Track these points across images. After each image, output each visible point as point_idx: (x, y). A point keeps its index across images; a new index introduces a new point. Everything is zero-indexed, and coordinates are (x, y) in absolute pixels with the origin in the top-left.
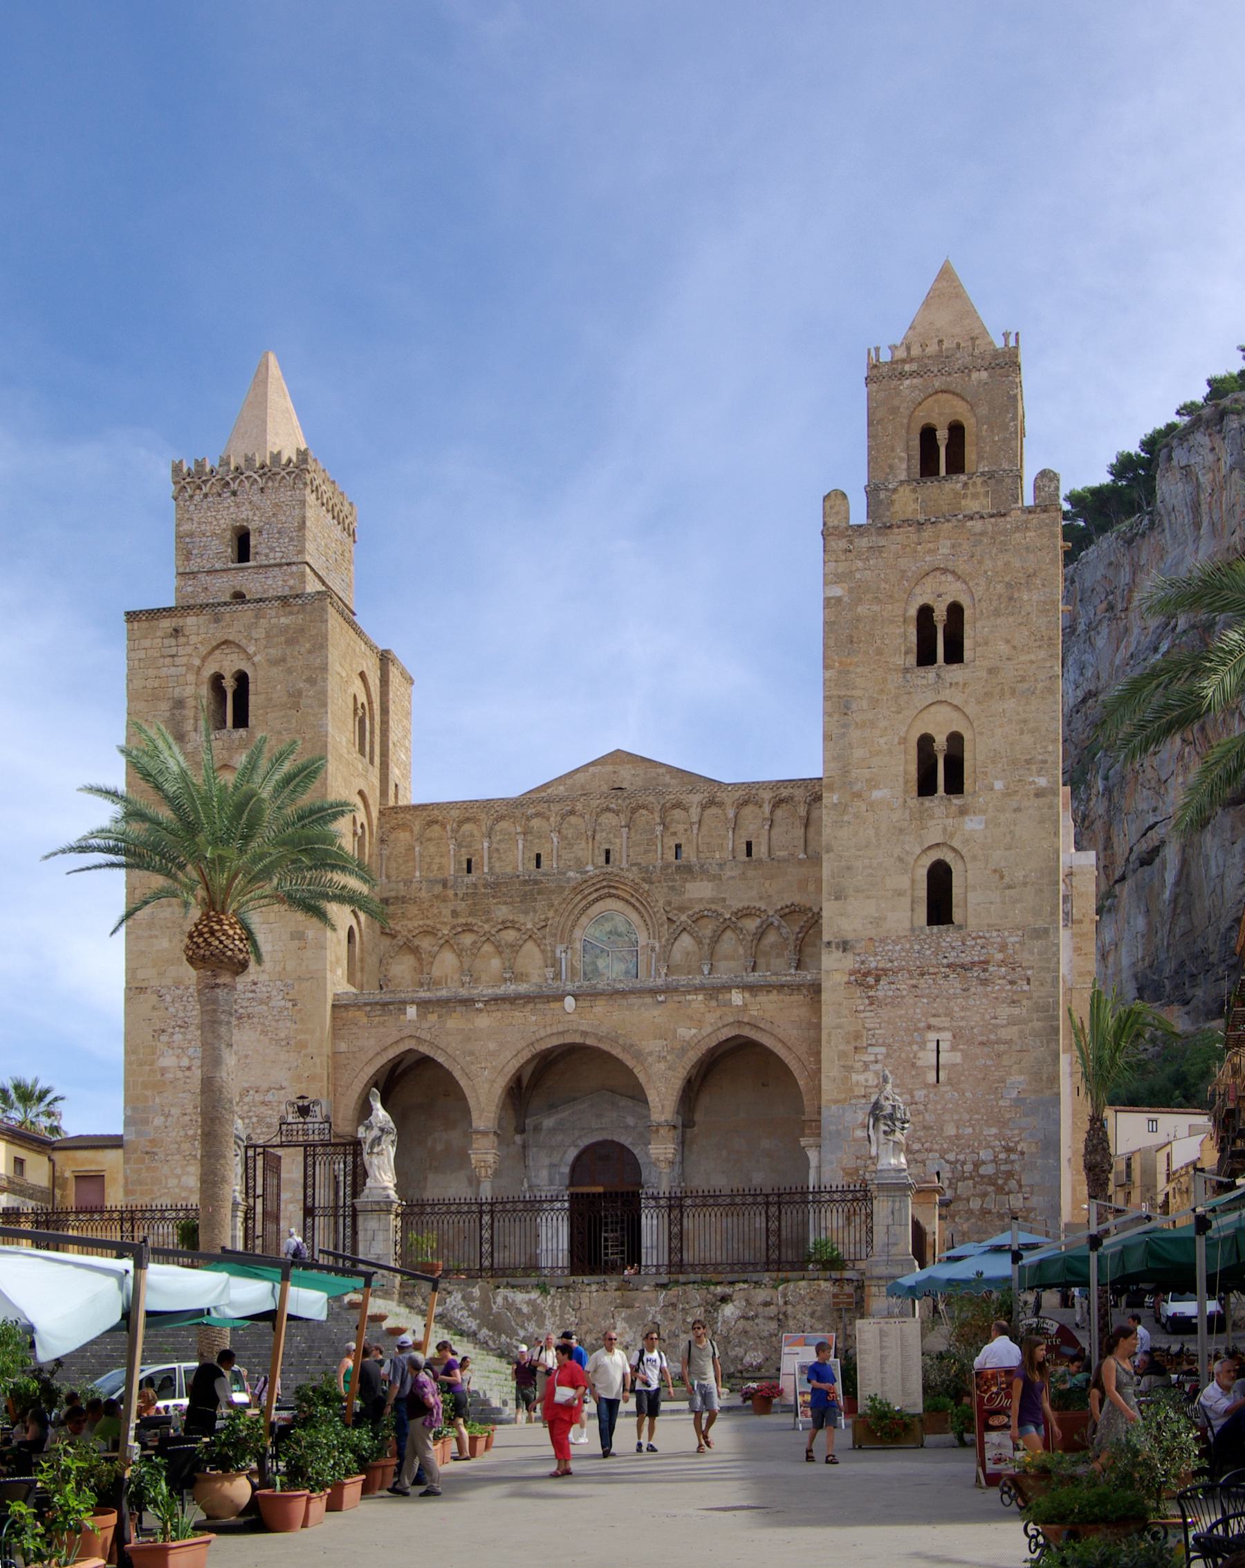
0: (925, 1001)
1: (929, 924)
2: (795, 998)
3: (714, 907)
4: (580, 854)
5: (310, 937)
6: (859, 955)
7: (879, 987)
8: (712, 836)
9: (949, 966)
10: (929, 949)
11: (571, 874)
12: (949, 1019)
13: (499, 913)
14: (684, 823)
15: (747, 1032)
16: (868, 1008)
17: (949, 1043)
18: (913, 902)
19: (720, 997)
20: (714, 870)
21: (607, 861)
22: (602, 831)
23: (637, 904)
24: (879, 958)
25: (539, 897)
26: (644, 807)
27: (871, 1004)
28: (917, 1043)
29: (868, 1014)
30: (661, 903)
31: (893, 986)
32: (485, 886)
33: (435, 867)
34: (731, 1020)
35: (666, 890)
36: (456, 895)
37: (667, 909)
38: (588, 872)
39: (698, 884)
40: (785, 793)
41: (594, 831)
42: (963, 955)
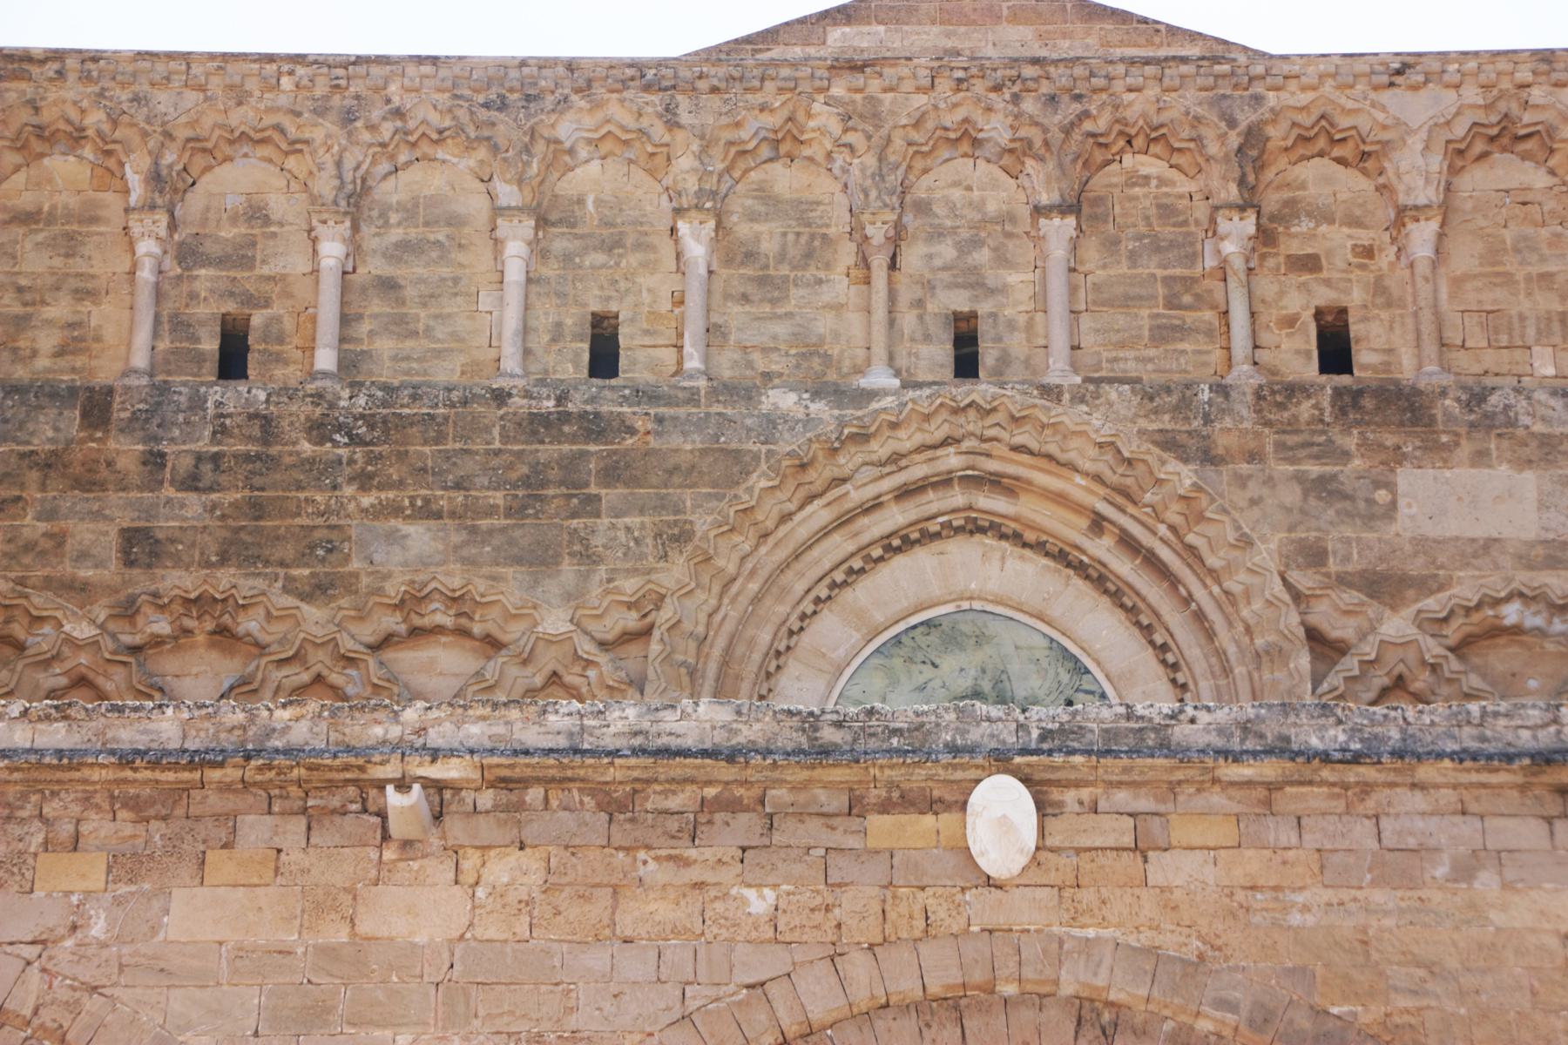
4: (824, 325)
8: (1508, 279)
11: (783, 400)
13: (389, 558)
14: (1354, 222)
21: (966, 366)
22: (937, 234)
23: (1124, 567)
25: (610, 495)
26: (1156, 137)
30: (1267, 553)
32: (319, 430)
33: (47, 341)
35: (1291, 495)
36: (155, 461)
37: (1304, 580)
38: (872, 395)
39: (1462, 475)
41: (897, 239)
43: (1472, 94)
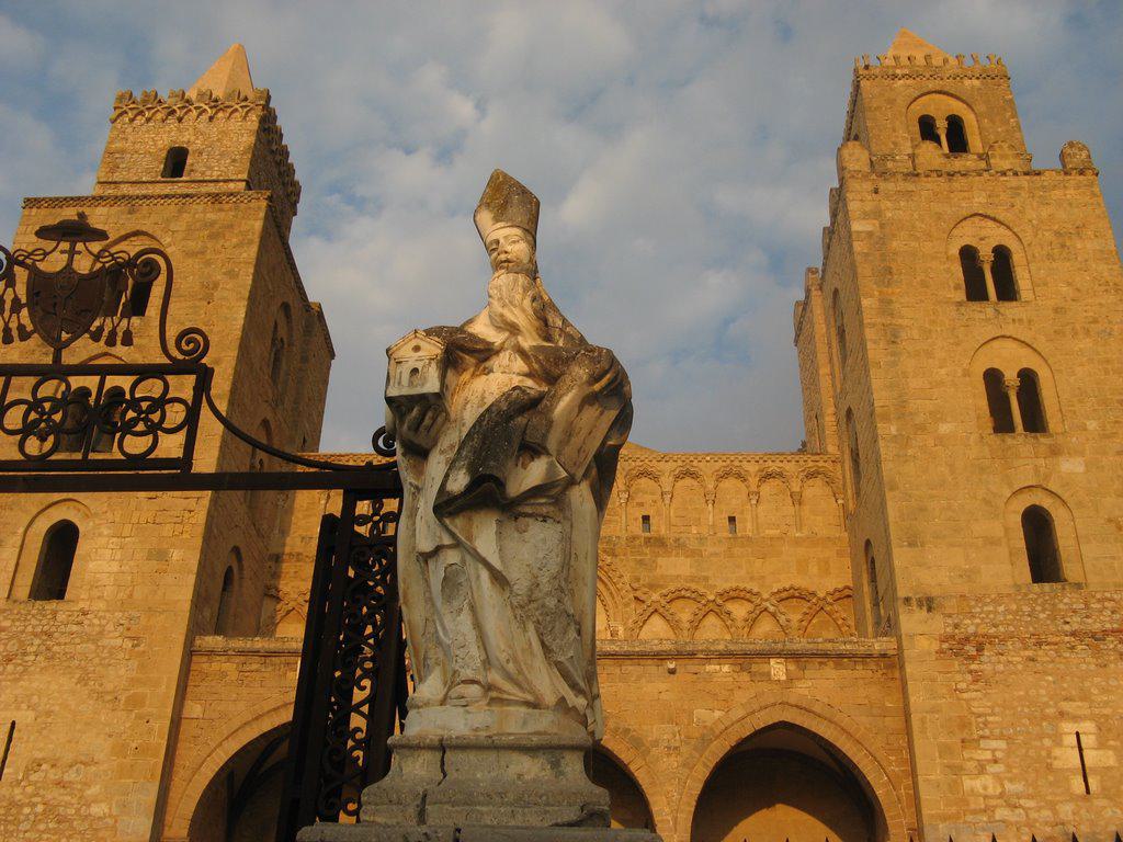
0: (1050, 678)
1: (1035, 580)
2: (860, 671)
3: (693, 586)
5: (175, 558)
6: (950, 616)
7: (982, 659)
9: (1073, 634)
10: (1043, 611)
12: (1086, 704)
15: (790, 716)
16: (972, 687)
17: (1093, 737)
18: (1011, 554)
19: (754, 668)
20: (693, 544)
24: (978, 621)
27: (976, 681)
28: (1049, 737)
29: (974, 694)
30: (626, 579)
31: (1002, 658)
34: (772, 701)
35: (632, 564)
37: (636, 585)
40: (773, 467)
42: (1090, 621)
43: (680, 463)
